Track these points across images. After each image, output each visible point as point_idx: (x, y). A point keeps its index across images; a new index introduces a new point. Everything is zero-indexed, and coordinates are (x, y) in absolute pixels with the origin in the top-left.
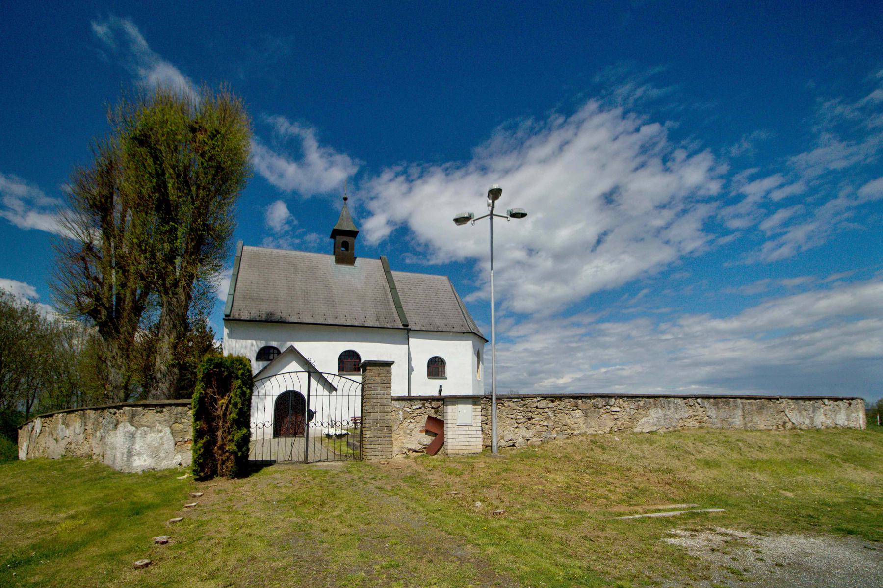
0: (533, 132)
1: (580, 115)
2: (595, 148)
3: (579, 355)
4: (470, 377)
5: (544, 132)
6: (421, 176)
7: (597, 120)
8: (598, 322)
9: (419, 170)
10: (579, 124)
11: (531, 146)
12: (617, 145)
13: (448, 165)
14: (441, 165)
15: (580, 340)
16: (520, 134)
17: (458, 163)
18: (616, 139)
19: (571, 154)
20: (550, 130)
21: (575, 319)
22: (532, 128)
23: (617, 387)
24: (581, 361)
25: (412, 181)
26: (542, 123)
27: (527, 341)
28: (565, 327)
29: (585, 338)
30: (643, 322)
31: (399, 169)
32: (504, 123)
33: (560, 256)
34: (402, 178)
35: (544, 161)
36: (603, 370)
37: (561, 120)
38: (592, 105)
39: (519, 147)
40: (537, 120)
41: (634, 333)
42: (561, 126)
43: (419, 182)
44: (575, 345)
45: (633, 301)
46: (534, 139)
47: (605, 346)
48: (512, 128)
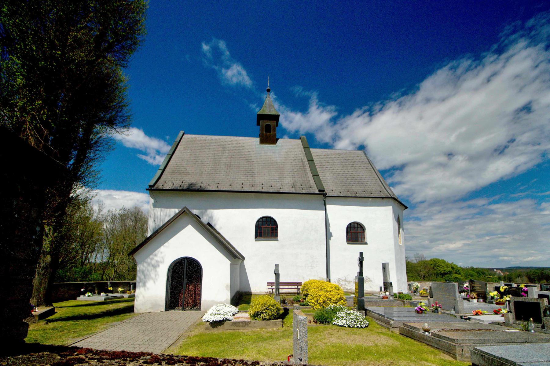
0: (468, 69)
1: (511, 52)
2: (517, 76)
3: (472, 227)
4: (392, 242)
5: (479, 68)
6: (381, 110)
7: (524, 53)
8: (490, 204)
9: (381, 106)
10: (508, 60)
11: (465, 80)
12: (536, 72)
13: (402, 99)
14: (396, 100)
15: (473, 218)
16: (459, 71)
17: (410, 97)
18: (537, 66)
19: (496, 83)
20: (484, 66)
21: (471, 202)
22: (470, 66)
23: (496, 250)
24: (471, 232)
25: (373, 115)
26: (477, 62)
27: (432, 219)
28: (461, 208)
29: (477, 216)
30: (527, 202)
31: (366, 108)
32: (450, 65)
33: (473, 158)
34: (367, 113)
35: (476, 89)
36: (487, 238)
37: (496, 56)
38: (522, 43)
39: (456, 82)
40: (474, 61)
41: (519, 211)
42: (492, 62)
43: (379, 114)
44: (468, 221)
45: (522, 188)
46: (469, 74)
47: (493, 220)
48: (454, 68)
